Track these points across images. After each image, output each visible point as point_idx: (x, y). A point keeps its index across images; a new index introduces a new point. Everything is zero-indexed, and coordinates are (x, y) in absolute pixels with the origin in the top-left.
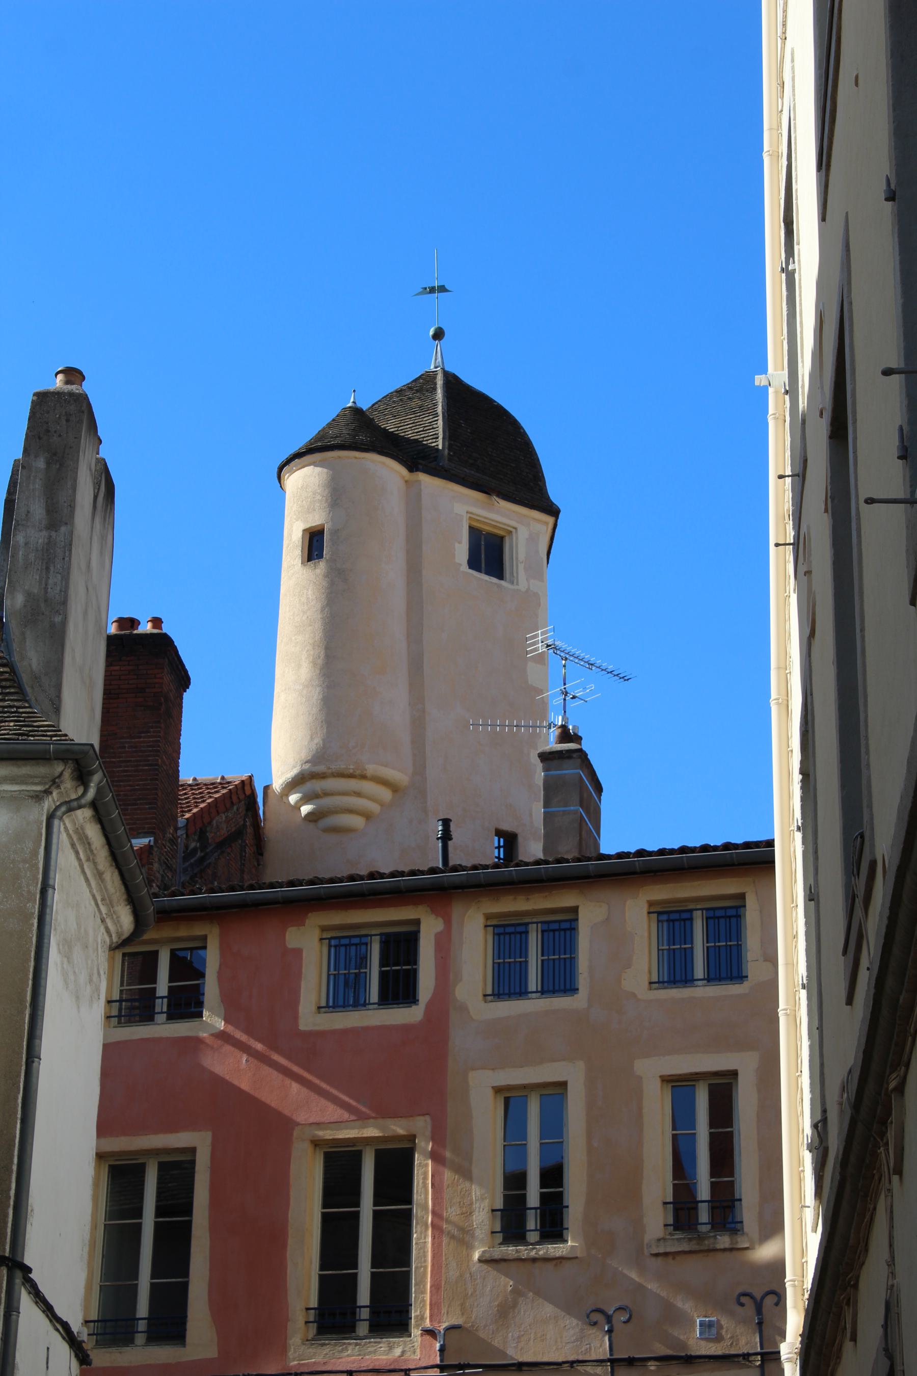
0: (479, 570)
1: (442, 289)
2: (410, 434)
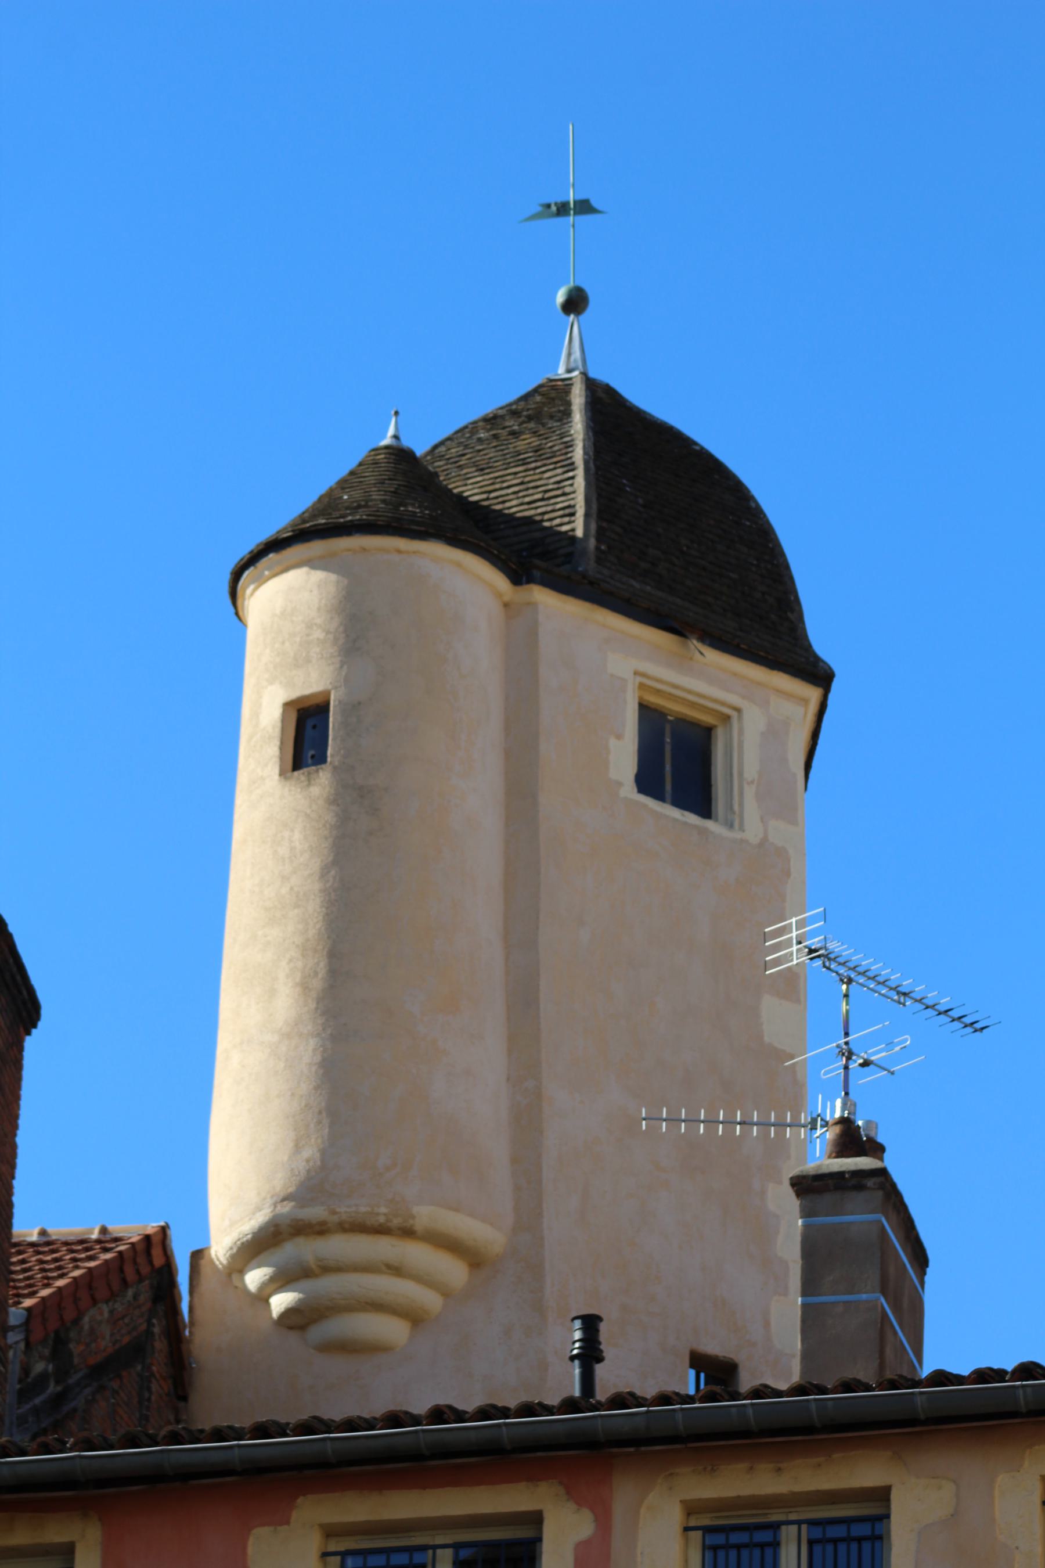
0: (659, 796)
1: (584, 207)
2: (514, 507)
